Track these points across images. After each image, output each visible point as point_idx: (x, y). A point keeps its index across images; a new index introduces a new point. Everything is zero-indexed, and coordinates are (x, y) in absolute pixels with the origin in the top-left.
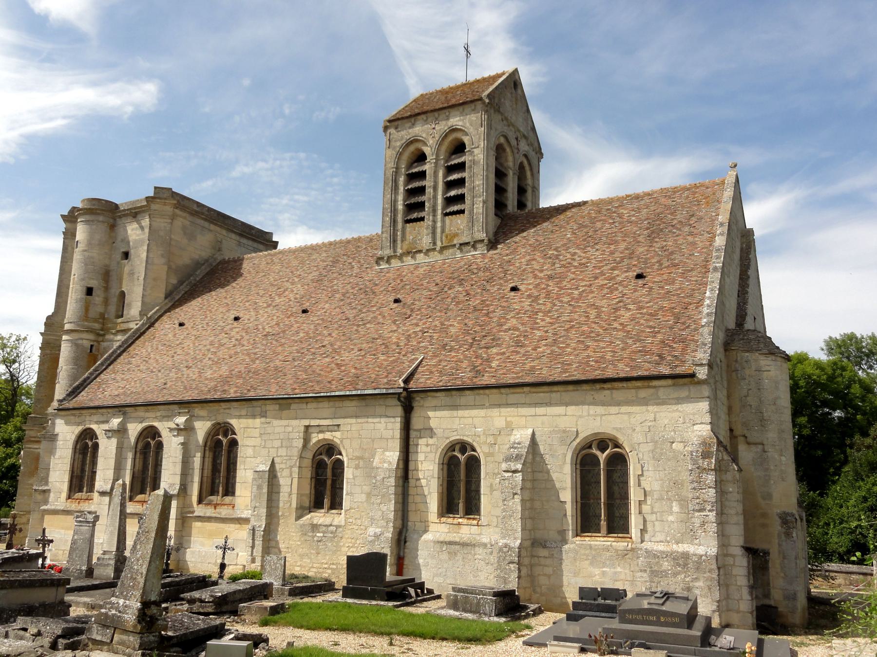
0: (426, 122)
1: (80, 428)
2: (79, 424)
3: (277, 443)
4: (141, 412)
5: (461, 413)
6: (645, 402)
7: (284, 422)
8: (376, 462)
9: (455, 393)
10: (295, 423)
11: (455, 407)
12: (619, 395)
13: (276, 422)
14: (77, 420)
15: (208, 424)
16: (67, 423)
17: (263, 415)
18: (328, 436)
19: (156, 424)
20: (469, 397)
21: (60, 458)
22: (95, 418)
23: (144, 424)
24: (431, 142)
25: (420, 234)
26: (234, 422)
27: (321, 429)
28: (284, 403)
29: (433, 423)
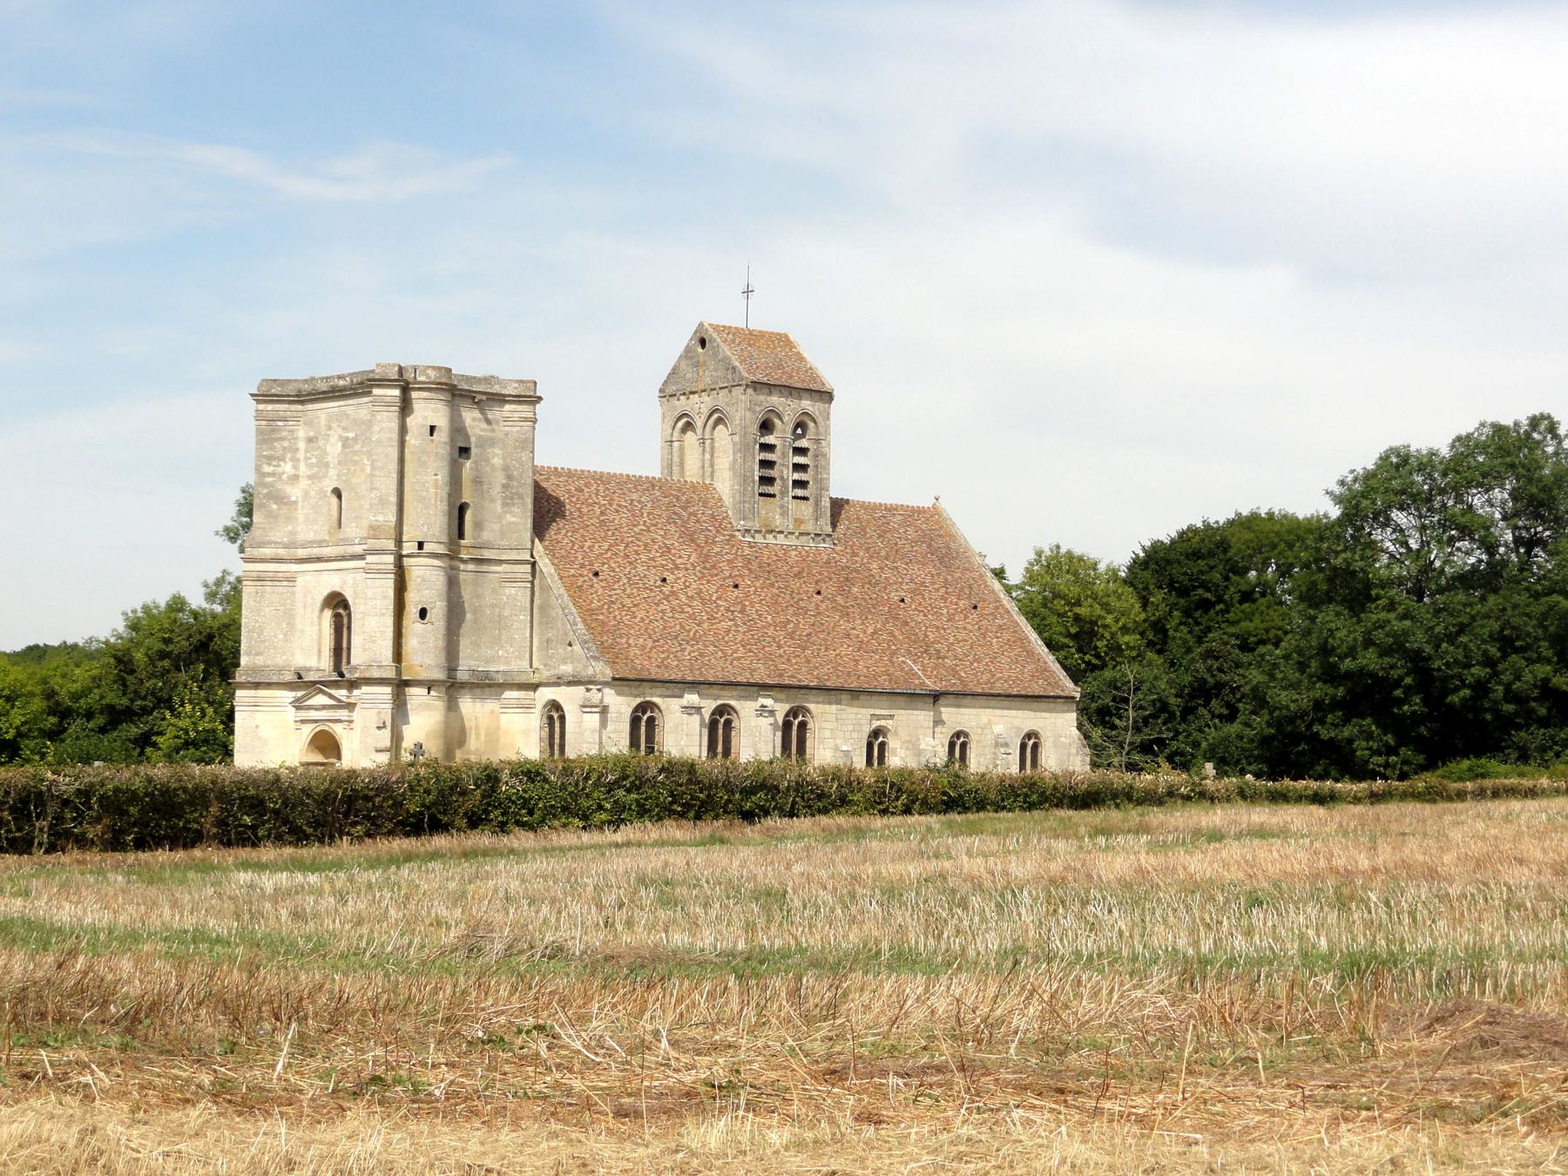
0: (781, 395)
1: (639, 700)
2: (636, 696)
3: (850, 728)
4: (715, 691)
5: (963, 710)
6: (1051, 711)
7: (855, 710)
8: (923, 746)
9: (963, 696)
10: (863, 711)
11: (958, 706)
12: (1042, 705)
13: (850, 710)
14: (634, 691)
15: (787, 707)
16: (618, 694)
17: (838, 702)
18: (883, 723)
19: (732, 703)
20: (968, 700)
21: (615, 731)
22: (659, 691)
23: (720, 702)
24: (786, 419)
25: (771, 512)
26: (811, 706)
27: (879, 717)
28: (857, 695)
29: (944, 717)
